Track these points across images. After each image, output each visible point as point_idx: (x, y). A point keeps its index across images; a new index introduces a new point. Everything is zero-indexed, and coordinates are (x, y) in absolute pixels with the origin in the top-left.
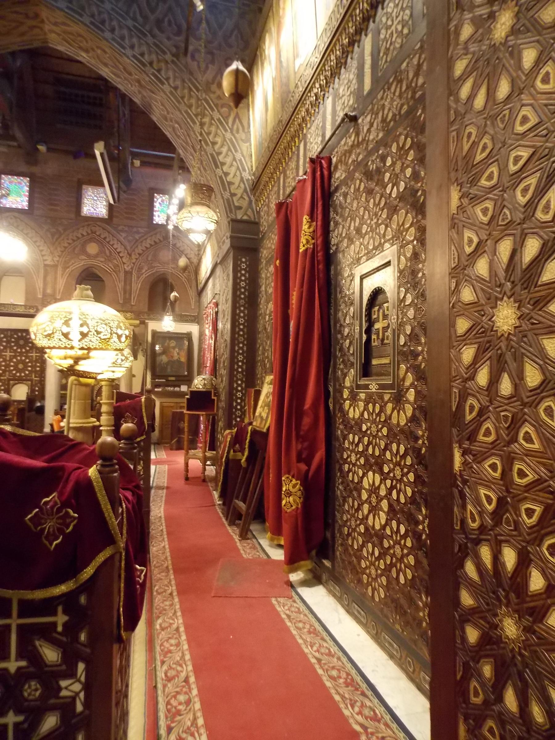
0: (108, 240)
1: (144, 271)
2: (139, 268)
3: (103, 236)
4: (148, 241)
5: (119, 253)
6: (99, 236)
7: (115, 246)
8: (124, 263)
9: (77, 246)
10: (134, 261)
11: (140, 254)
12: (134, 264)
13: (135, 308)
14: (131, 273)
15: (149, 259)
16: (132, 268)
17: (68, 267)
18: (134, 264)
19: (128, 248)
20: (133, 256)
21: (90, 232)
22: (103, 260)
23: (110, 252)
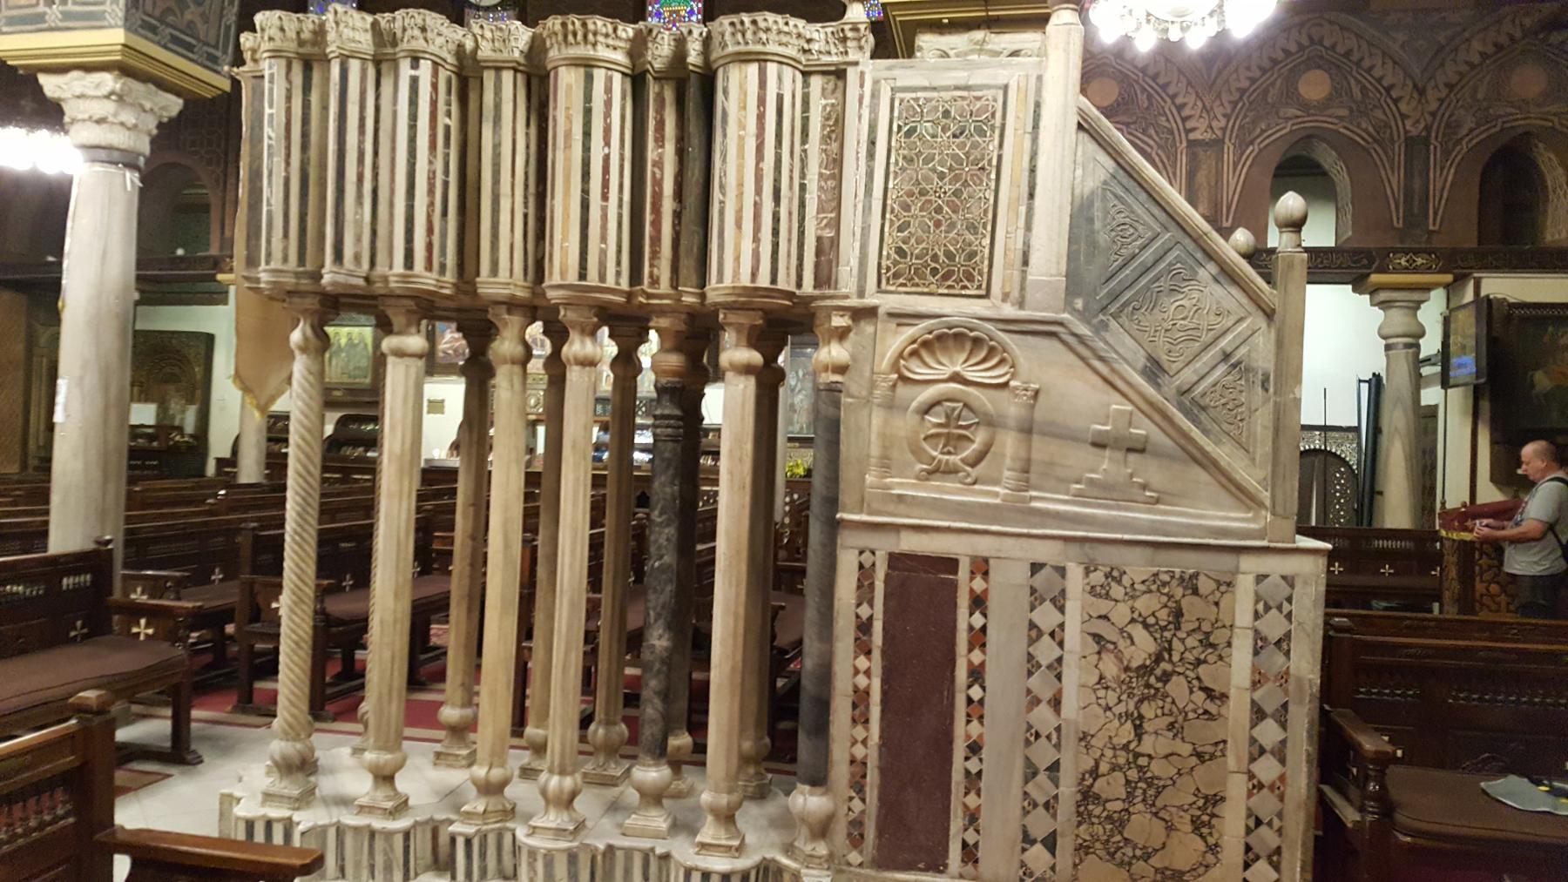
0: (1355, 57)
1: (1465, 132)
2: (1448, 125)
3: (1340, 49)
4: (1477, 45)
5: (1388, 90)
6: (1333, 47)
7: (1377, 72)
8: (1404, 117)
9: (1273, 84)
10: (1434, 106)
11: (1450, 86)
12: (1433, 114)
13: (1436, 243)
14: (1426, 142)
15: (1480, 96)
16: (1428, 128)
17: (1252, 143)
18: (1433, 114)
19: (1417, 71)
20: (1431, 94)
21: (1305, 42)
22: (1344, 112)
23: (1363, 89)
